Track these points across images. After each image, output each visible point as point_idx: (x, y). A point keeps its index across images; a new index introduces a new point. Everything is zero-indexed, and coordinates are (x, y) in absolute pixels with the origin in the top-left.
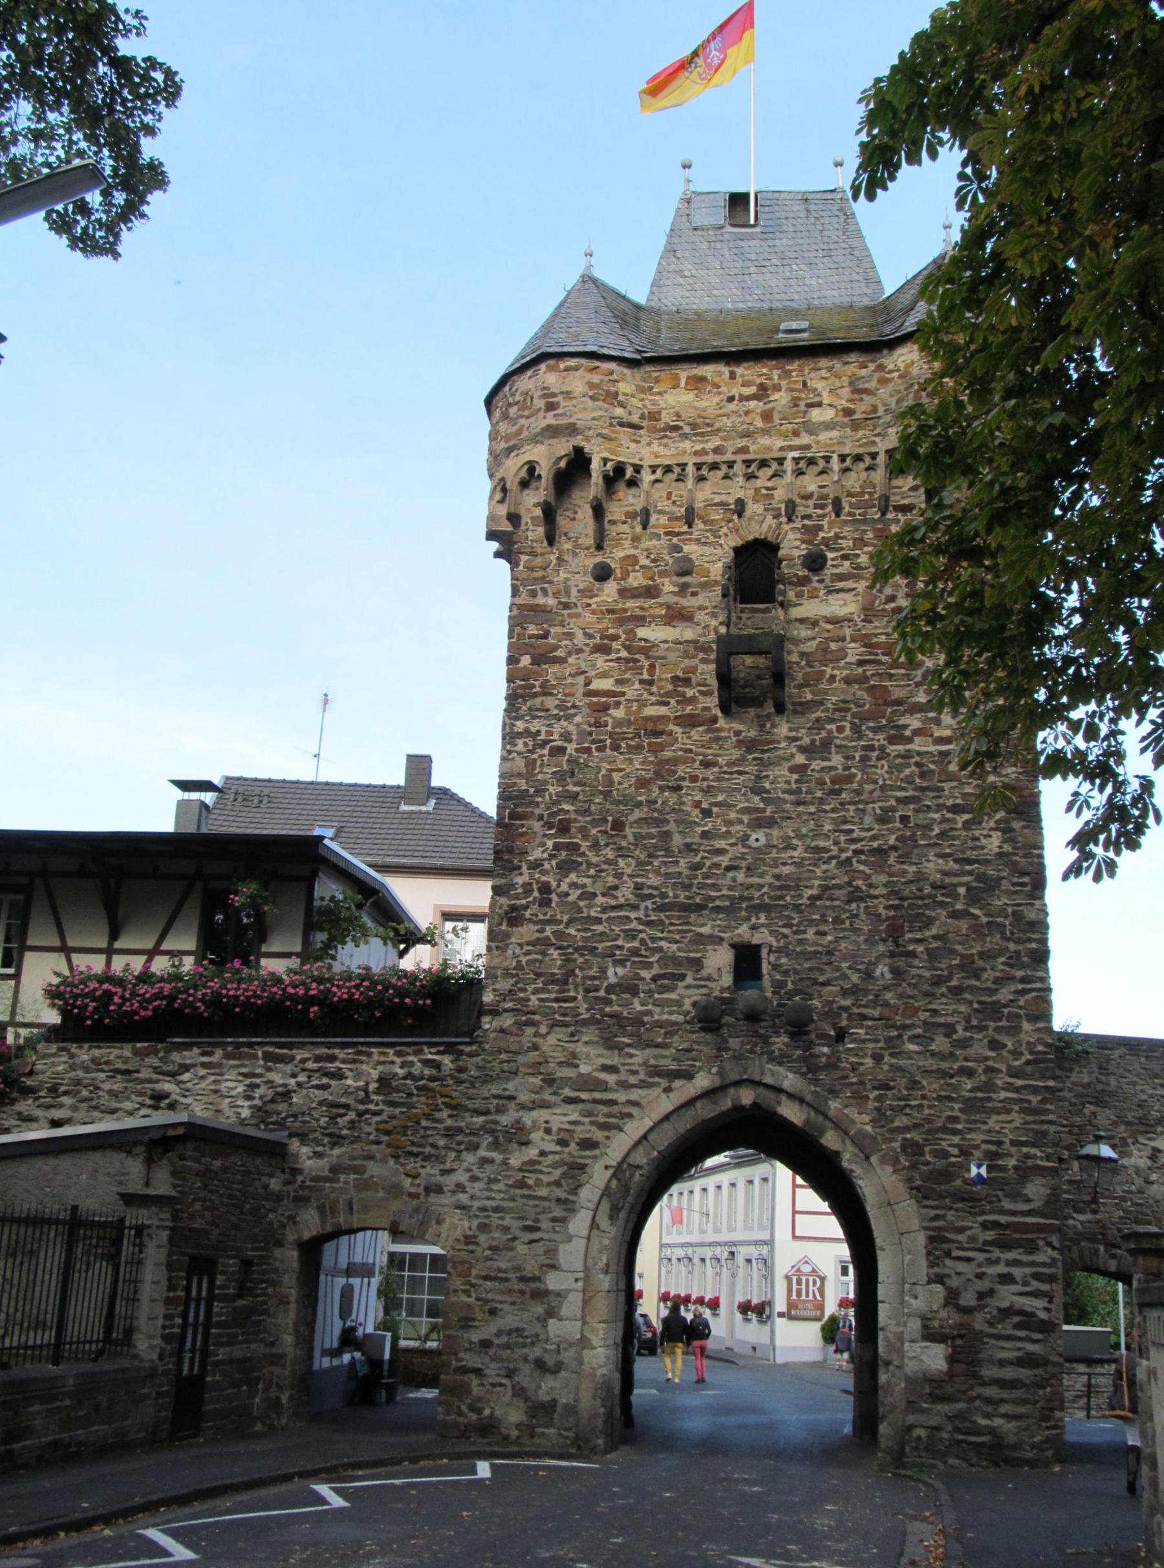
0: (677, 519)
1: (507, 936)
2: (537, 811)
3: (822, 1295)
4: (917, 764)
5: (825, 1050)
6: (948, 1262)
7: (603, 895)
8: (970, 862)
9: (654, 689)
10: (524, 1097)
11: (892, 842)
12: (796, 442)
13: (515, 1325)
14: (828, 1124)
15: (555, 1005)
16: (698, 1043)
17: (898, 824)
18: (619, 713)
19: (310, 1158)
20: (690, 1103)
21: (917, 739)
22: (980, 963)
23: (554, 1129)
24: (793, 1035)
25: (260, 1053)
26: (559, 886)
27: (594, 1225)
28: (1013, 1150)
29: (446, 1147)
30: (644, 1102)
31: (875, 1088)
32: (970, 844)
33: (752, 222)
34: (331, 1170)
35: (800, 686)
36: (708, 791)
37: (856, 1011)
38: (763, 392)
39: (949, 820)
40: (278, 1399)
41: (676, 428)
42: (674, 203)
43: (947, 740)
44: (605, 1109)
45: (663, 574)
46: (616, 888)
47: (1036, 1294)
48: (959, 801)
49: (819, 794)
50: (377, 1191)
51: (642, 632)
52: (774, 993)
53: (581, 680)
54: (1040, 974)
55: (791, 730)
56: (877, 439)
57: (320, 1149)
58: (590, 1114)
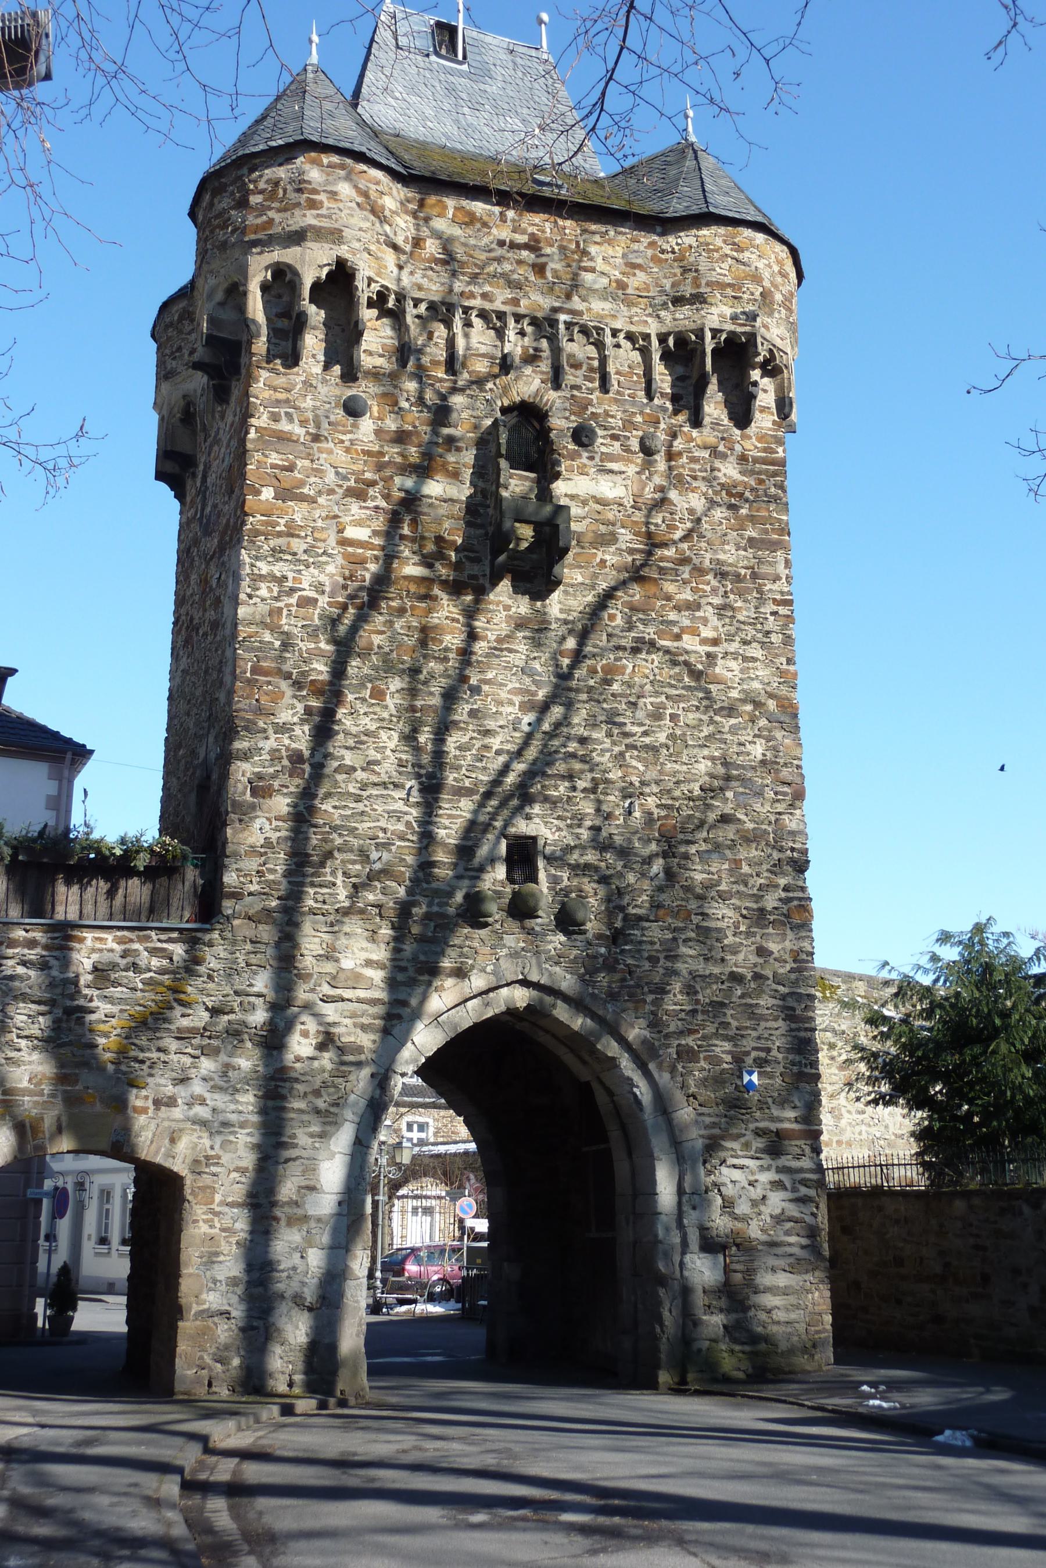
7: (363, 769)
21: (685, 637)
31: (651, 992)
33: (460, 57)
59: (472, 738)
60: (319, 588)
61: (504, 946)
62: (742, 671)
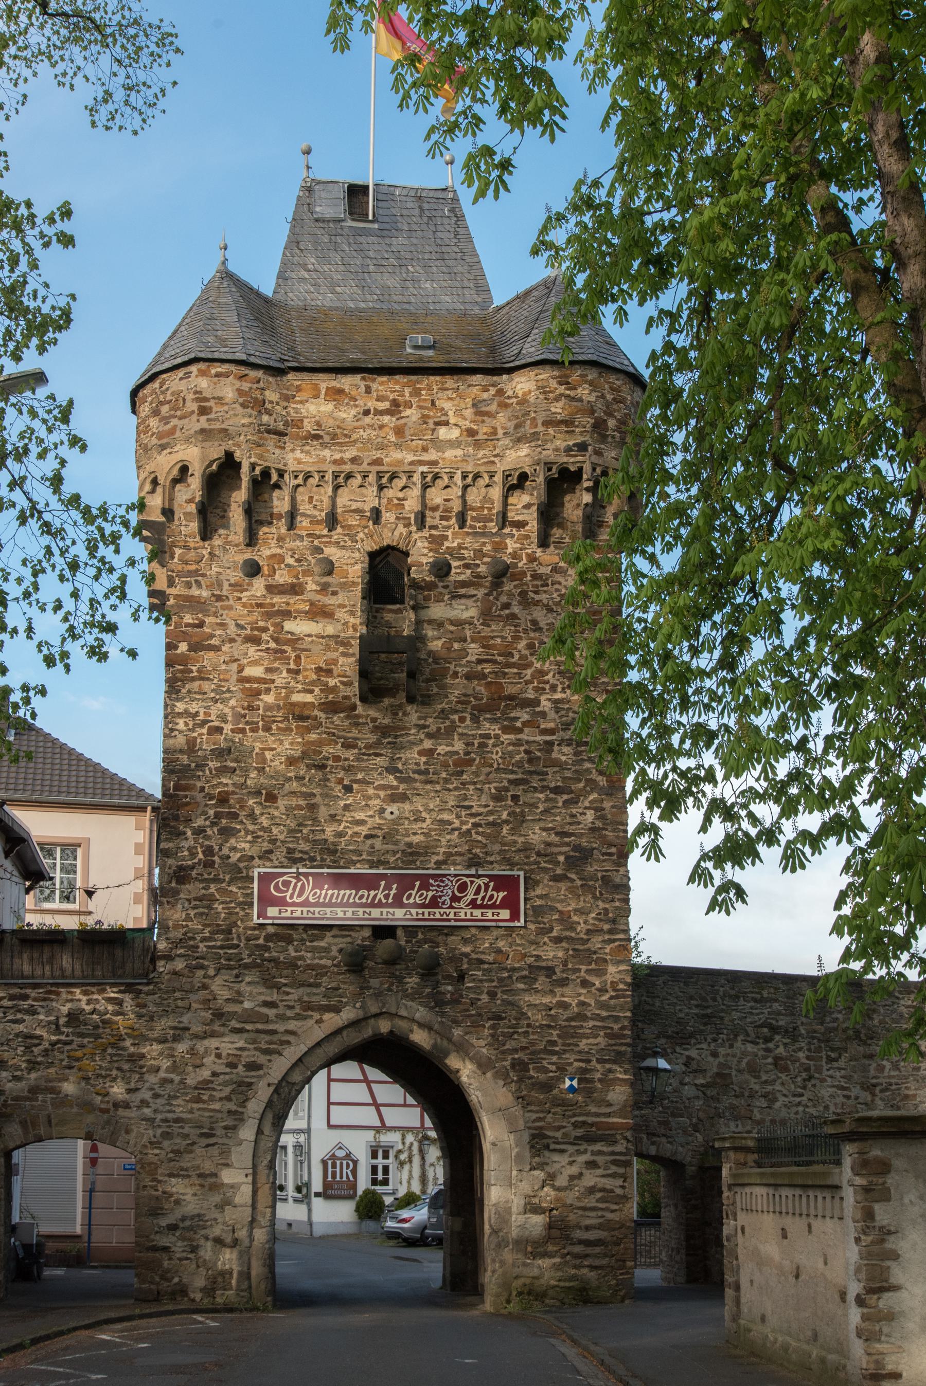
0: (318, 522)
1: (176, 893)
2: (199, 784)
4: (526, 752)
5: (450, 988)
6: (546, 1153)
8: (569, 835)
9: (300, 678)
10: (197, 1028)
11: (504, 816)
12: (426, 457)
13: (196, 1212)
14: (451, 1047)
18: (269, 699)
20: (338, 1032)
21: (526, 730)
22: (575, 918)
24: (422, 976)
27: (259, 1132)
28: (599, 1066)
29: (130, 1070)
30: (299, 1031)
32: (568, 819)
35: (428, 681)
36: (348, 770)
37: (474, 956)
38: (395, 408)
41: (317, 437)
42: (295, 191)
43: (552, 732)
44: (268, 1038)
45: (306, 573)
47: (614, 1176)
49: (444, 775)
51: (289, 626)
53: (234, 667)
54: (622, 927)
55: (420, 718)
56: (496, 460)
57: (18, 1073)
58: (254, 1042)
60: (223, 718)
61: (369, 988)
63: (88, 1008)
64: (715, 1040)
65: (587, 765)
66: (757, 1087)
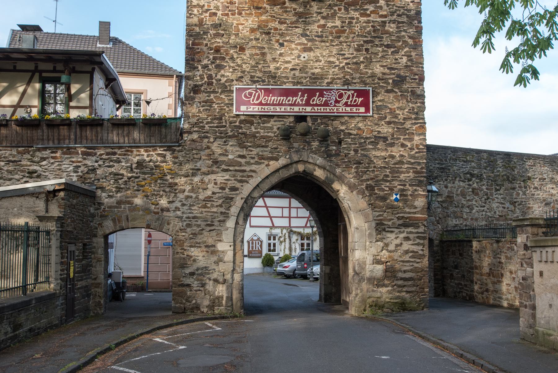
1: (193, 98)
2: (205, 42)
3: (261, 248)
4: (372, 26)
5: (334, 148)
6: (384, 233)
10: (204, 169)
11: (362, 59)
13: (204, 265)
15: (217, 129)
16: (281, 145)
17: (364, 52)
19: (107, 198)
21: (372, 15)
22: (398, 112)
23: (219, 183)
25: (80, 152)
26: (216, 76)
27: (237, 223)
28: (410, 188)
29: (170, 192)
30: (257, 171)
31: (354, 164)
32: (394, 61)
34: (117, 203)
36: (282, 35)
37: (346, 131)
39: (385, 51)
40: (100, 302)
43: (385, 16)
44: (241, 174)
46: (242, 77)
47: (418, 244)
48: (389, 43)
49: (331, 38)
50: (139, 211)
52: (312, 124)
54: (421, 117)
55: (318, 9)
57: (111, 194)
58: (234, 176)
59: (280, 65)
60: (217, 8)
62: (397, 28)
63: (148, 159)
64: (446, 180)
65: (403, 33)
66: (465, 203)
